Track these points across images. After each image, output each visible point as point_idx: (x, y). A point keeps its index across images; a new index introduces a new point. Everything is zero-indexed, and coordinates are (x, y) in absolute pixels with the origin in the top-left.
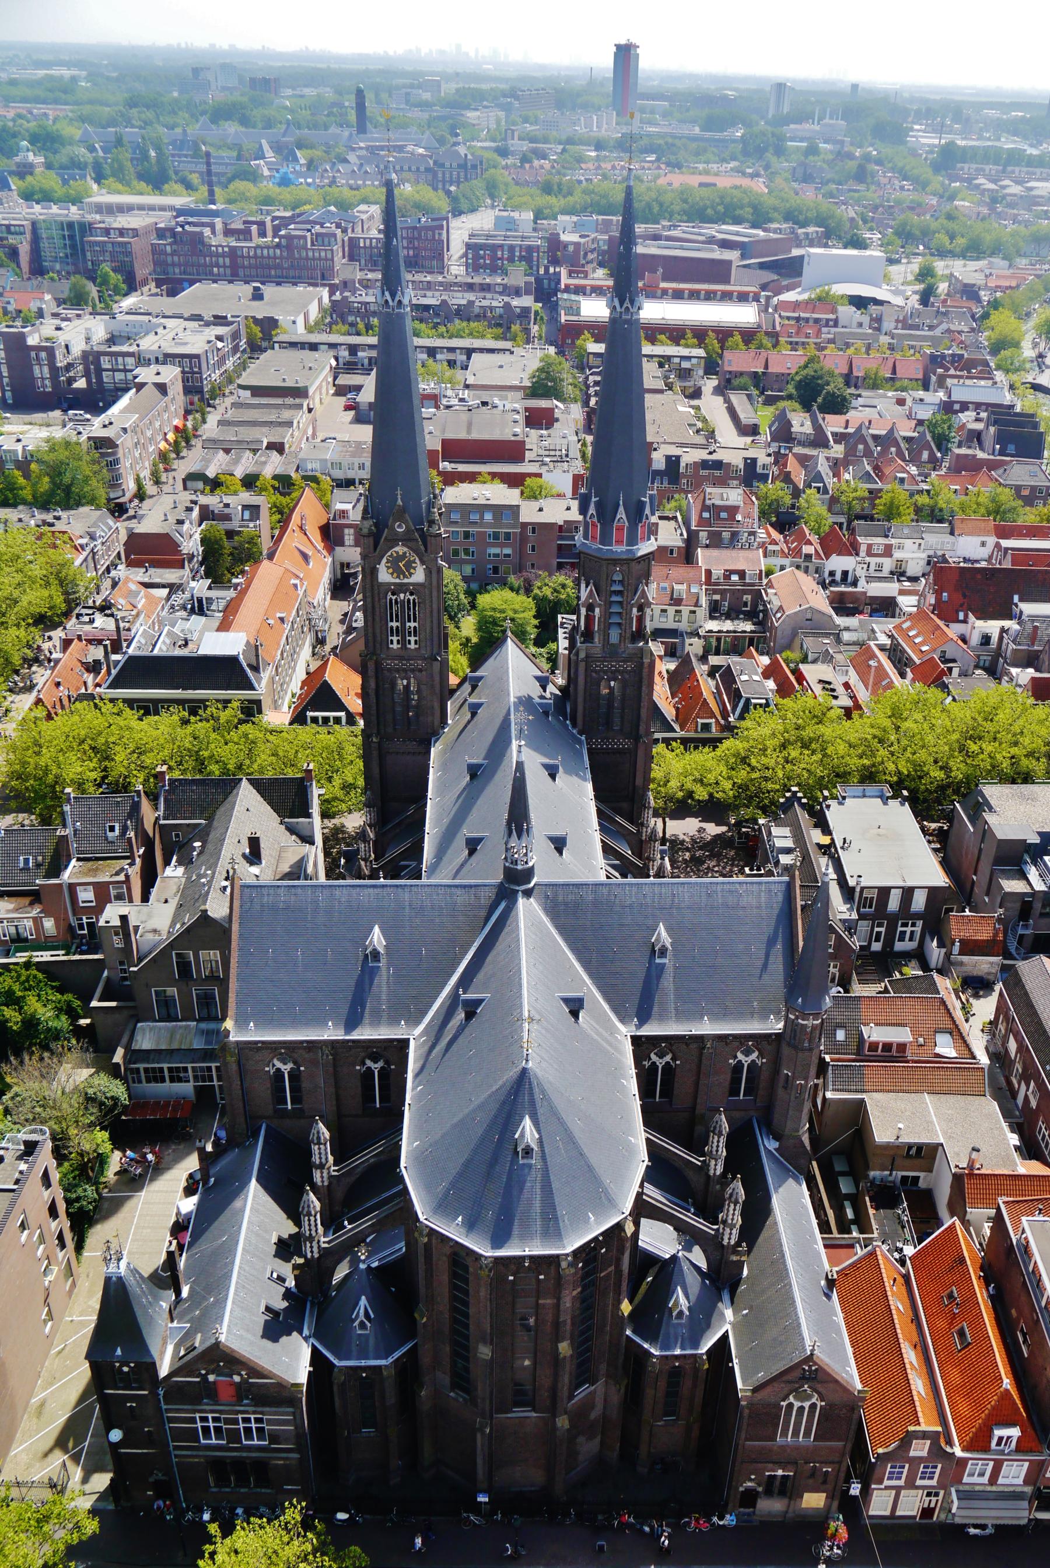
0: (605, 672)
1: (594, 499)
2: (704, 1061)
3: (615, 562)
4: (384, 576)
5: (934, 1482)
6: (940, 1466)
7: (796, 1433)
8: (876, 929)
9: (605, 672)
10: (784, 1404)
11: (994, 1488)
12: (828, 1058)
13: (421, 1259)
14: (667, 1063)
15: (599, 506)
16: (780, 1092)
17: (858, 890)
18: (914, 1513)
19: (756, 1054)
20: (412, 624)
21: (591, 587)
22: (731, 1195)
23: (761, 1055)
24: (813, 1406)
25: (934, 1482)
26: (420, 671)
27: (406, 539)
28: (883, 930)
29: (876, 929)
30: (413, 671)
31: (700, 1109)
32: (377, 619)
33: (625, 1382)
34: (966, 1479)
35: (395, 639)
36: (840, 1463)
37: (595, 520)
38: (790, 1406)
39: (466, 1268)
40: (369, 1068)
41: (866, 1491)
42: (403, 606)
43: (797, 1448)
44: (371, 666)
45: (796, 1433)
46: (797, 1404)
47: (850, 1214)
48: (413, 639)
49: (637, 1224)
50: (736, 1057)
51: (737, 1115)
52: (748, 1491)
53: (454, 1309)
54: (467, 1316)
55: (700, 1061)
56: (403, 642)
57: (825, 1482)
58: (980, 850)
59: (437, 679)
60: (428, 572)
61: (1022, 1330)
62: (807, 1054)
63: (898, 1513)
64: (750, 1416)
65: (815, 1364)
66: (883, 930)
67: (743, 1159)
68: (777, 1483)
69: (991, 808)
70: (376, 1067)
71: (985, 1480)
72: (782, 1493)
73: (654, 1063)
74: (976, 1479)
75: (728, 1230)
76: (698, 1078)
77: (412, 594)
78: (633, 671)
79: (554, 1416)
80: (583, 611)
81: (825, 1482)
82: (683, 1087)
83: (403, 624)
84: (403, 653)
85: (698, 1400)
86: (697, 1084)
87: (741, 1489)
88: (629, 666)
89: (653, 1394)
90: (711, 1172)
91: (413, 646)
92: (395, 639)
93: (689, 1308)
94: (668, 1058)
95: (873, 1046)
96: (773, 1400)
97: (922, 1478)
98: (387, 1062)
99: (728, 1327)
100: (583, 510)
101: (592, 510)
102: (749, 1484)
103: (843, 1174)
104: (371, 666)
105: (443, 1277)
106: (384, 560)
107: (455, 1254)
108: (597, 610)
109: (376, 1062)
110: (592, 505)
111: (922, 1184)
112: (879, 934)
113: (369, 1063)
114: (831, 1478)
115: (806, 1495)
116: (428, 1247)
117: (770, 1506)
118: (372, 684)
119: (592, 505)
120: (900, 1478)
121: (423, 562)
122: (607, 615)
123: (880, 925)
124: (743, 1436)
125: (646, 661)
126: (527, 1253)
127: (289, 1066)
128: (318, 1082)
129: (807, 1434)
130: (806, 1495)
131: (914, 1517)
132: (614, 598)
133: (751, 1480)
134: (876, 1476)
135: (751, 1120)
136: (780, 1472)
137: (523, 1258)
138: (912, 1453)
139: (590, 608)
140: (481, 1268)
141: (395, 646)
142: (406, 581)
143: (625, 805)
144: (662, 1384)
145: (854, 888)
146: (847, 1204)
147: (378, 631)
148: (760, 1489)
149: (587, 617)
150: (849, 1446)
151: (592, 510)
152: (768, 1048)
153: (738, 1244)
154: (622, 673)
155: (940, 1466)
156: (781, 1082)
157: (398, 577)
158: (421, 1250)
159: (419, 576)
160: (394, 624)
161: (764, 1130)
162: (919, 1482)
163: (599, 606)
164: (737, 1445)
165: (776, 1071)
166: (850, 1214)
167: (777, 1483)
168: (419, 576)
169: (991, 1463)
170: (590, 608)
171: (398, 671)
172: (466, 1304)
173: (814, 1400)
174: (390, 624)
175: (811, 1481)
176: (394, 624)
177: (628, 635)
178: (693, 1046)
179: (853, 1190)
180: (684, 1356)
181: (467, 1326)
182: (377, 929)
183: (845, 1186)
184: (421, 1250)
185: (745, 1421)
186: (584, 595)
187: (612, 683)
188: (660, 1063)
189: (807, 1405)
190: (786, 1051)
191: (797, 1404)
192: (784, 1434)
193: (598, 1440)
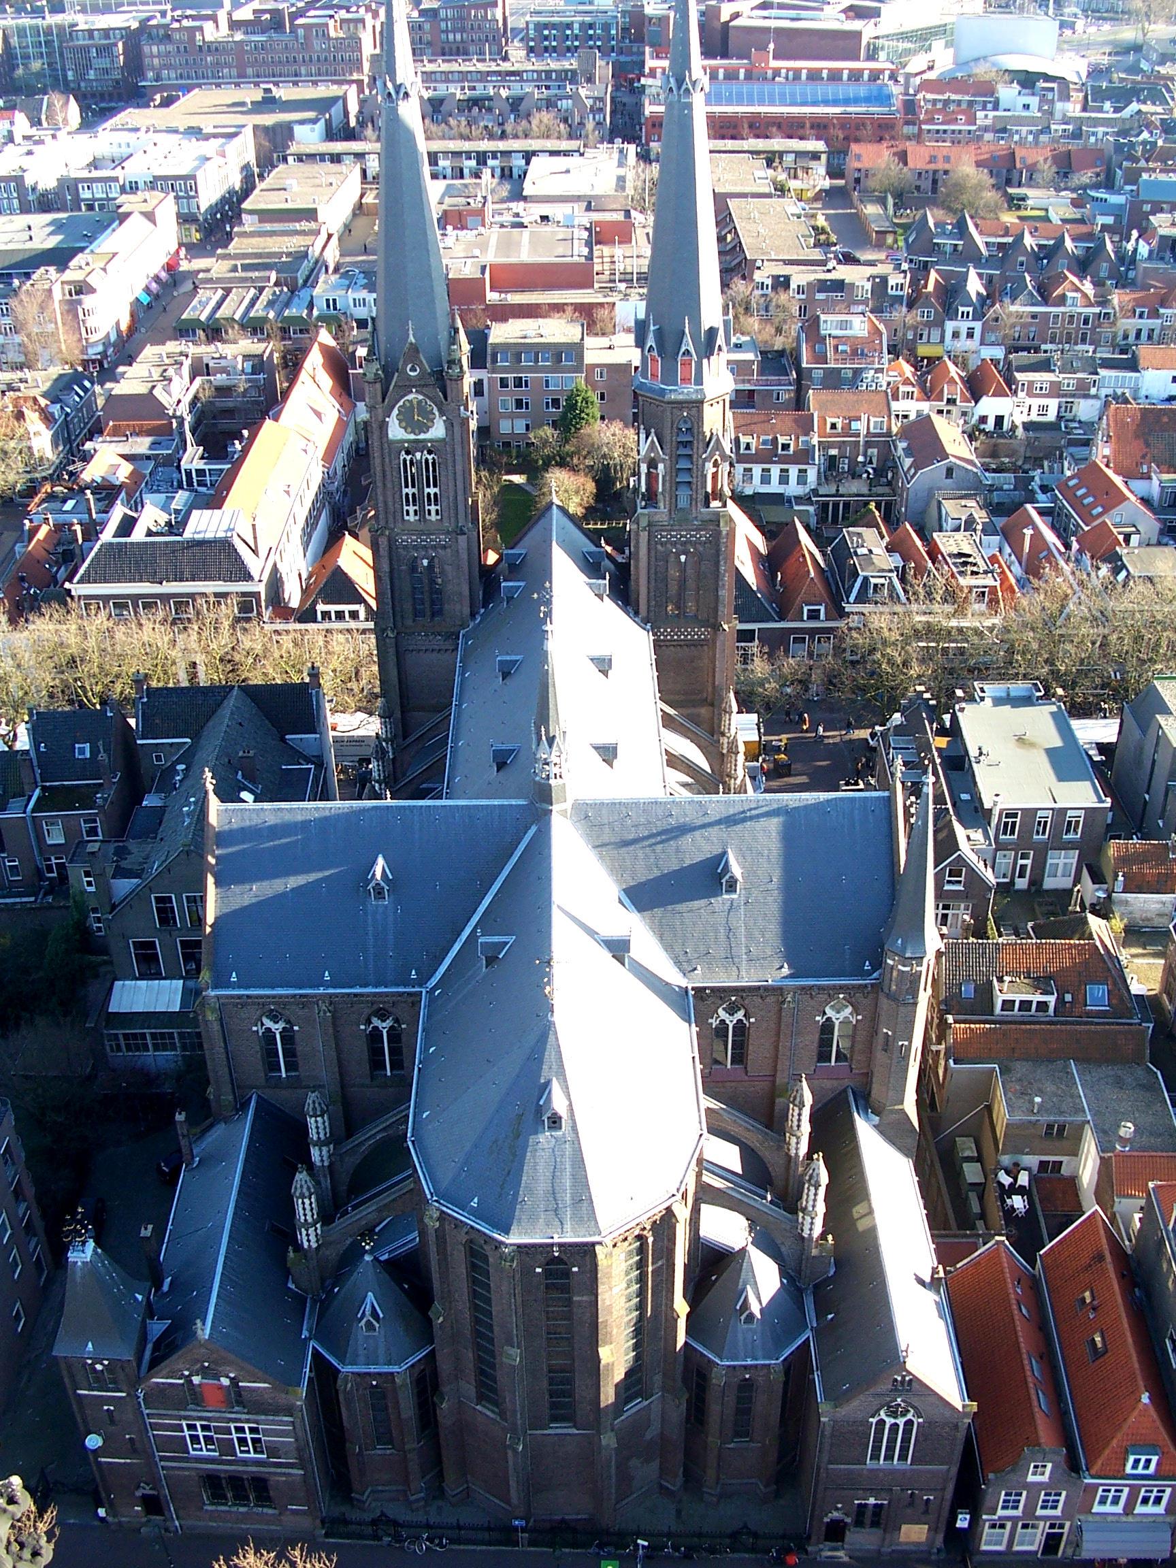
0: (674, 544)
1: (652, 328)
2: (784, 1019)
3: (680, 404)
4: (396, 431)
5: (1058, 1512)
6: (1064, 1493)
7: (889, 1457)
8: (1021, 862)
9: (674, 544)
10: (873, 1420)
11: (1130, 1519)
12: (950, 1019)
13: (433, 1248)
14: (740, 1021)
15: (659, 335)
16: (880, 1056)
17: (996, 812)
18: (1033, 1548)
19: (850, 1009)
20: (432, 490)
21: (653, 437)
22: (811, 1176)
23: (856, 1011)
24: (909, 1423)
25: (1058, 1512)
26: (444, 547)
27: (420, 386)
28: (1028, 862)
29: (1021, 862)
30: (434, 548)
31: (780, 1079)
32: (389, 485)
33: (686, 1396)
34: (1096, 1508)
35: (411, 509)
36: (943, 1489)
37: (655, 353)
38: (881, 1423)
39: (485, 1259)
40: (376, 1028)
41: (975, 1521)
42: (419, 469)
43: (893, 1472)
44: (383, 542)
45: (889, 1457)
46: (889, 1421)
47: (976, 1208)
48: (433, 508)
49: (696, 1211)
50: (824, 1013)
51: (828, 1084)
52: (834, 1522)
53: (476, 1308)
54: (489, 1314)
55: (780, 1018)
56: (421, 513)
57: (926, 1512)
58: (1154, 761)
59: (464, 556)
60: (449, 426)
61: (1171, 1338)
62: (910, 1008)
63: (1016, 1548)
64: (832, 1435)
65: (909, 1373)
66: (1028, 862)
67: (833, 1137)
68: (869, 1513)
69: (1166, 711)
70: (384, 1026)
71: (1119, 1509)
72: (875, 1524)
73: (723, 1021)
74: (1108, 1508)
75: (808, 1219)
76: (778, 1041)
77: (430, 452)
78: (708, 541)
79: (599, 1433)
80: (644, 468)
81: (926, 1512)
82: (758, 1049)
83: (421, 490)
84: (422, 526)
85: (775, 1418)
86: (777, 1048)
87: (826, 1520)
88: (703, 535)
89: (719, 1410)
90: (793, 1153)
91: (433, 517)
92: (411, 509)
93: (762, 1310)
94: (740, 1015)
95: (1008, 1005)
96: (860, 1416)
97: (1043, 1507)
98: (397, 1020)
99: (809, 1333)
100: (640, 343)
101: (651, 342)
102: (835, 1515)
103: (969, 1159)
104: (383, 542)
105: (460, 1268)
106: (395, 411)
107: (471, 1241)
108: (661, 466)
109: (383, 1021)
110: (651, 335)
111: (1065, 1171)
112: (1023, 867)
113: (376, 1022)
114: (931, 1506)
115: (904, 1528)
116: (440, 1235)
117: (862, 1539)
118: (386, 567)
119: (651, 335)
120: (1016, 1508)
121: (442, 413)
122: (674, 471)
123: (1024, 857)
124: (825, 1458)
125: (724, 529)
126: (556, 1240)
127: (281, 1025)
128: (317, 1049)
129: (903, 1457)
130: (904, 1528)
131: (1036, 1552)
132: (682, 451)
133: (837, 1509)
134: (988, 1503)
135: (845, 1091)
136: (872, 1501)
137: (552, 1245)
138: (1031, 1478)
139: (652, 464)
140: (501, 1258)
141: (412, 518)
142: (422, 436)
143: (704, 711)
144: (731, 1399)
145: (991, 810)
146: (973, 1196)
147: (390, 499)
148: (848, 1520)
149: (649, 474)
150: (954, 1470)
151: (651, 342)
152: (866, 1002)
153: (823, 1236)
154: (694, 544)
155: (1064, 1493)
156: (880, 1040)
157: (413, 432)
158: (432, 1239)
159: (438, 430)
160: (410, 491)
161: (861, 1102)
162: (1039, 1512)
163: (663, 461)
164: (819, 1468)
165: (874, 1032)
166: (976, 1208)
167: (869, 1513)
168: (438, 430)
169: (1126, 1490)
170: (652, 464)
171: (416, 548)
172: (488, 1301)
173: (909, 1416)
174: (405, 491)
175: (909, 1511)
176: (410, 491)
177: (701, 497)
178: (771, 1000)
179: (979, 1179)
180: (756, 1366)
181: (490, 1327)
182: (381, 861)
183: (972, 1172)
184: (432, 1239)
185: (827, 1441)
186: (644, 449)
187: (683, 558)
188: (731, 1021)
189: (901, 1421)
190: (884, 1003)
191: (889, 1421)
192: (875, 1457)
193: (655, 1465)
